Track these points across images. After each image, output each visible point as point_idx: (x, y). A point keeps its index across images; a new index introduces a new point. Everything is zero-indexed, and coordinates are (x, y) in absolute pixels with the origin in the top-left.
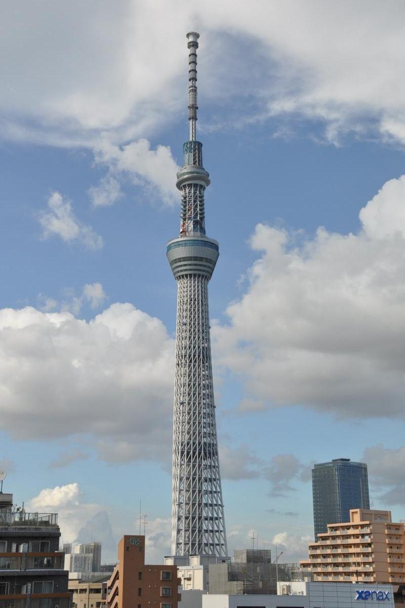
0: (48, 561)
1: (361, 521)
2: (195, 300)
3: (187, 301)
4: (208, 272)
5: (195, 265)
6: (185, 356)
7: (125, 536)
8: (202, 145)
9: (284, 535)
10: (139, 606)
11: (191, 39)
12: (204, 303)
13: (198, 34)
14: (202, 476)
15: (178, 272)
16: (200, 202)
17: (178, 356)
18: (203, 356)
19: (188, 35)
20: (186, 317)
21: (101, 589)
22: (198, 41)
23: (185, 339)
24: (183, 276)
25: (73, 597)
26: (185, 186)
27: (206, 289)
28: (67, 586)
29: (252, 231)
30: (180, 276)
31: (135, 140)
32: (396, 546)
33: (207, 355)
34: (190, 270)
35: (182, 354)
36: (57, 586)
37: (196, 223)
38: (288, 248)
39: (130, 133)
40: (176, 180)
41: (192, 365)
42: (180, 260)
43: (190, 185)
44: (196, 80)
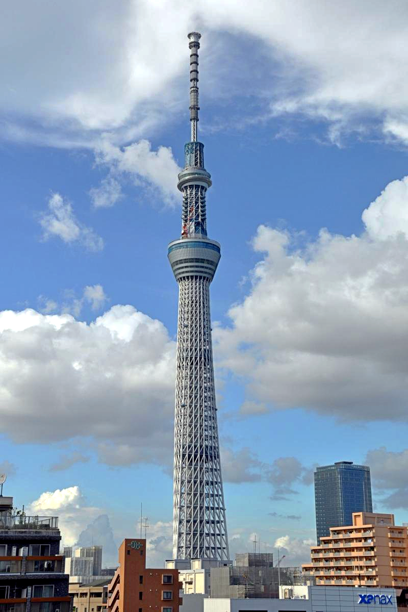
0: (48, 565)
1: (363, 524)
2: (197, 302)
3: (189, 303)
4: (209, 274)
5: (197, 267)
6: (187, 358)
7: (128, 541)
8: (203, 146)
9: (286, 538)
10: (140, 610)
11: (192, 39)
12: (206, 305)
13: (200, 34)
14: (203, 479)
15: (180, 274)
16: (202, 203)
17: (179, 358)
18: (205, 359)
19: (189, 36)
20: (187, 319)
21: (101, 593)
22: (200, 42)
23: (187, 342)
24: (184, 278)
25: (74, 601)
26: (186, 188)
27: (207, 291)
28: (68, 591)
29: (254, 233)
30: (181, 278)
31: (136, 141)
32: (399, 550)
33: (208, 357)
34: (192, 272)
35: (183, 356)
36: (58, 590)
37: (197, 224)
38: (290, 250)
39: (131, 134)
40: (177, 182)
41: (194, 368)
42: (181, 262)
43: (191, 187)
44: (197, 81)
